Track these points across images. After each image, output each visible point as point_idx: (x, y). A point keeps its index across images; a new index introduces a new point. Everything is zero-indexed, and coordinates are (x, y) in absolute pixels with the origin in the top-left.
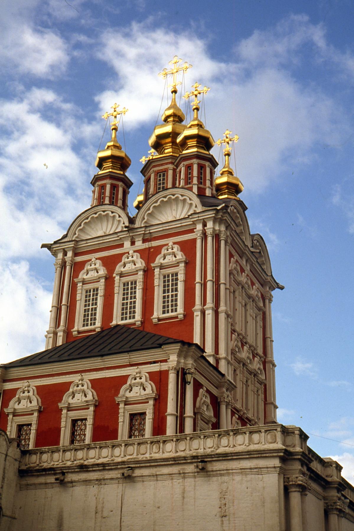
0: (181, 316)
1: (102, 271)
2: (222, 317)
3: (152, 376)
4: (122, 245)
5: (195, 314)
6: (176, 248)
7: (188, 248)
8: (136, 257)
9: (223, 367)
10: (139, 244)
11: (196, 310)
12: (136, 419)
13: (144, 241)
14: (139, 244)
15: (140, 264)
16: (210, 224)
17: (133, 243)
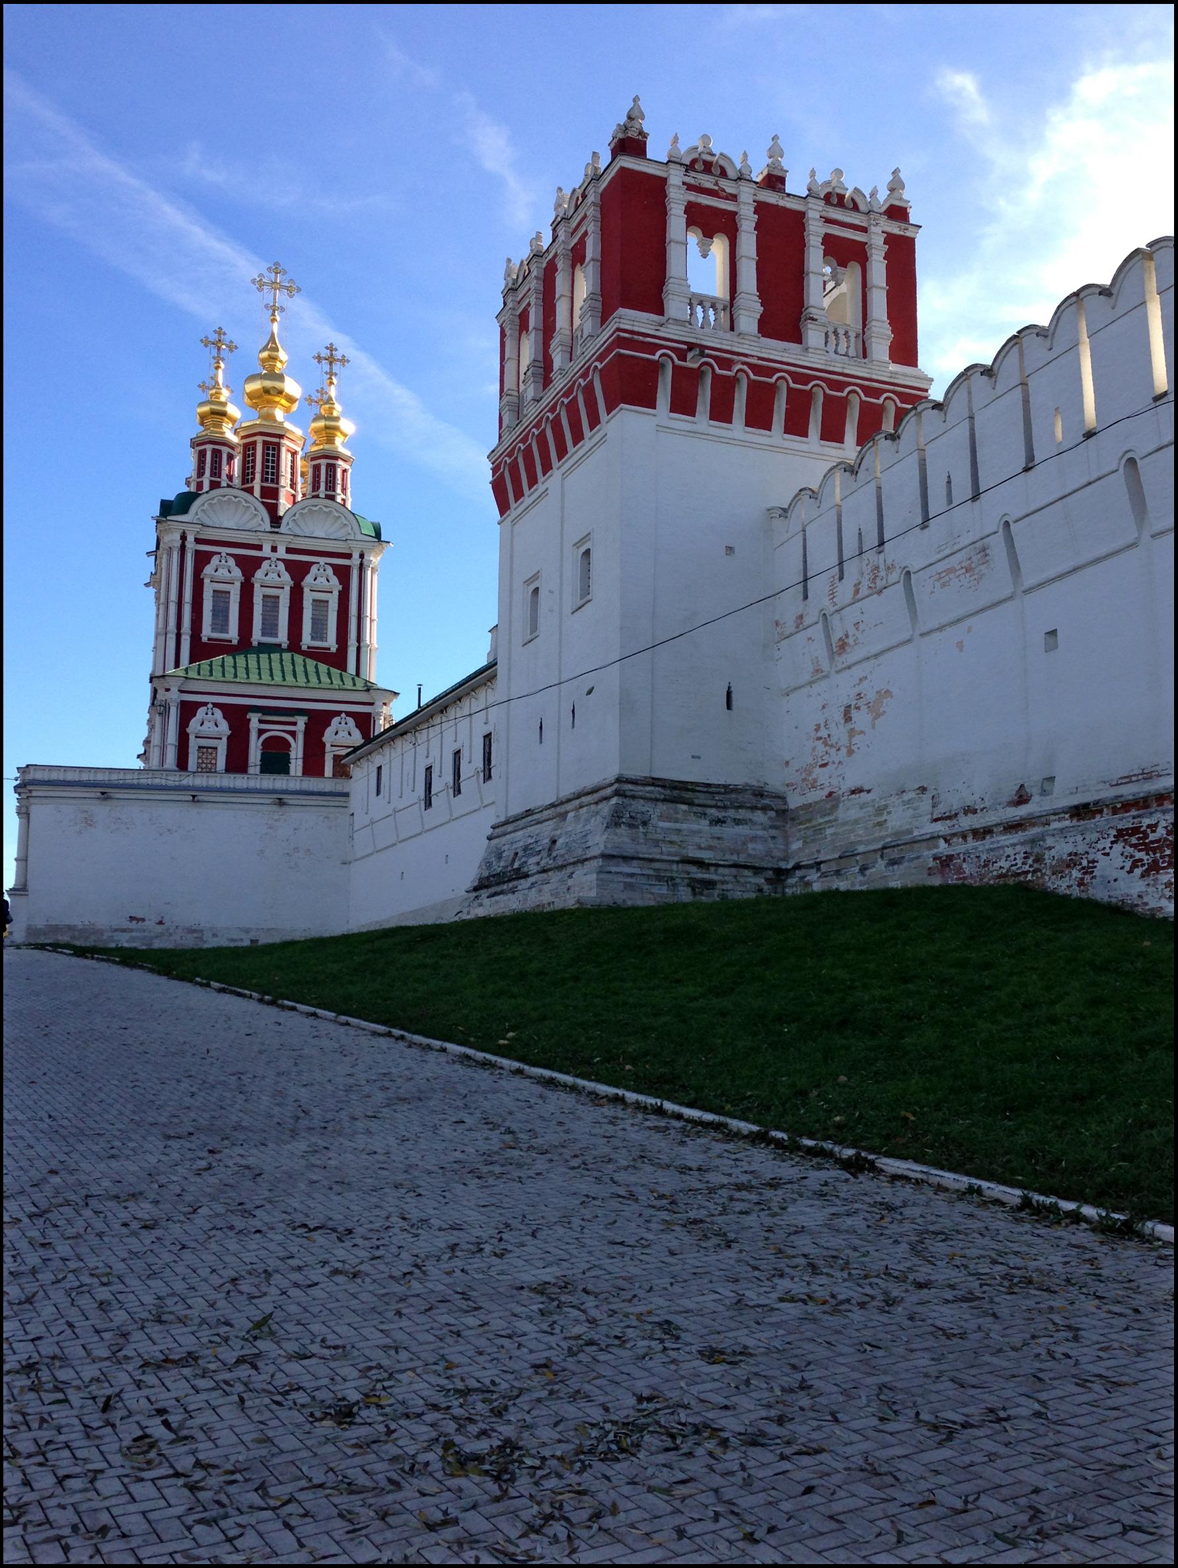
1: (237, 573)
6: (330, 570)
14: (281, 553)
17: (274, 549)
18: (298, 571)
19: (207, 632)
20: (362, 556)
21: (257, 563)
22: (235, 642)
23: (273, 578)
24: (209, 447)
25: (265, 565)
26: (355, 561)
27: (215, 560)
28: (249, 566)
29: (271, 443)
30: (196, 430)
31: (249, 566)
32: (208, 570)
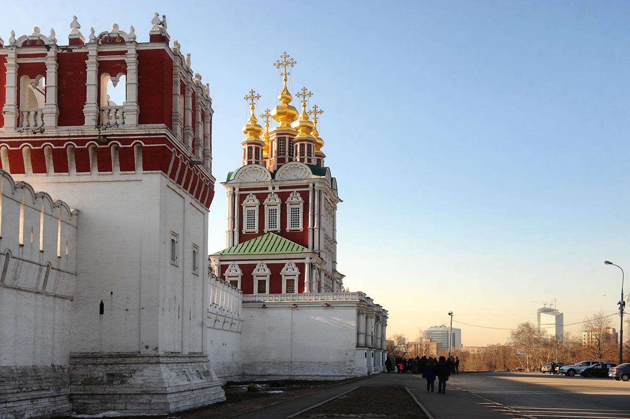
0: (301, 230)
1: (257, 201)
2: (322, 231)
3: (297, 265)
4: (267, 189)
5: (309, 230)
6: (298, 195)
7: (305, 195)
8: (276, 196)
9: (323, 255)
10: (277, 190)
11: (309, 228)
12: (290, 283)
13: (280, 188)
15: (278, 200)
16: (316, 185)
17: (274, 188)
18: (283, 196)
19: (245, 229)
20: (314, 185)
21: (266, 195)
22: (257, 232)
23: (273, 201)
24: (253, 146)
25: (269, 196)
26: (310, 189)
27: (248, 197)
28: (262, 197)
29: (281, 138)
30: (247, 137)
31: (262, 197)
32: (245, 202)
